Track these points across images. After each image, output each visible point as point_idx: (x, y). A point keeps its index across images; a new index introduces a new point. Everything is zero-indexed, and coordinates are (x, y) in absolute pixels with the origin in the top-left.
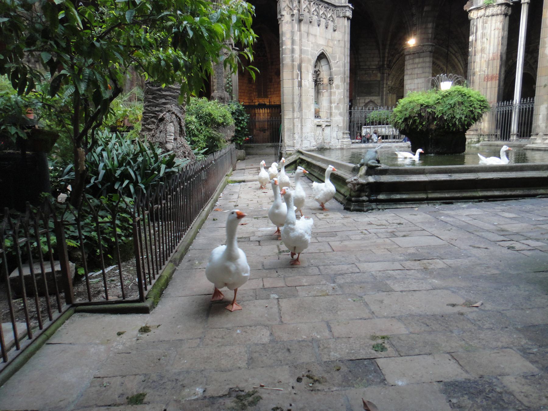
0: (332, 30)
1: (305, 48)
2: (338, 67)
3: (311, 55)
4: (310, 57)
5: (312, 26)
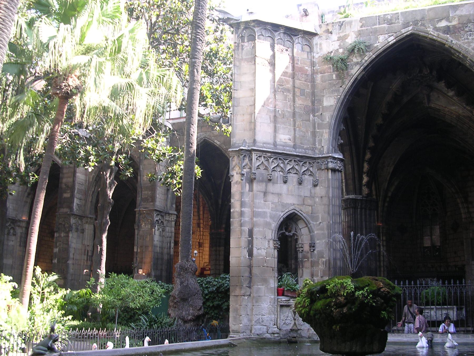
0: (310, 186)
1: (260, 210)
2: (322, 229)
3: (271, 217)
4: (268, 220)
5: (273, 183)
